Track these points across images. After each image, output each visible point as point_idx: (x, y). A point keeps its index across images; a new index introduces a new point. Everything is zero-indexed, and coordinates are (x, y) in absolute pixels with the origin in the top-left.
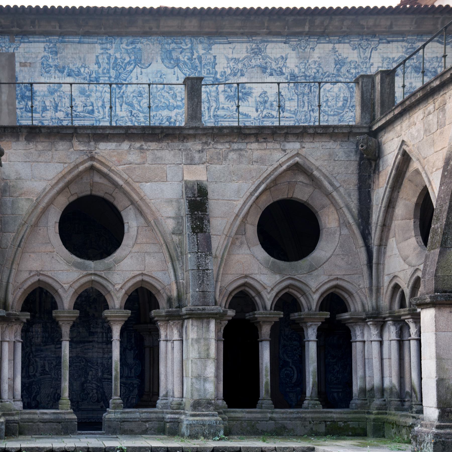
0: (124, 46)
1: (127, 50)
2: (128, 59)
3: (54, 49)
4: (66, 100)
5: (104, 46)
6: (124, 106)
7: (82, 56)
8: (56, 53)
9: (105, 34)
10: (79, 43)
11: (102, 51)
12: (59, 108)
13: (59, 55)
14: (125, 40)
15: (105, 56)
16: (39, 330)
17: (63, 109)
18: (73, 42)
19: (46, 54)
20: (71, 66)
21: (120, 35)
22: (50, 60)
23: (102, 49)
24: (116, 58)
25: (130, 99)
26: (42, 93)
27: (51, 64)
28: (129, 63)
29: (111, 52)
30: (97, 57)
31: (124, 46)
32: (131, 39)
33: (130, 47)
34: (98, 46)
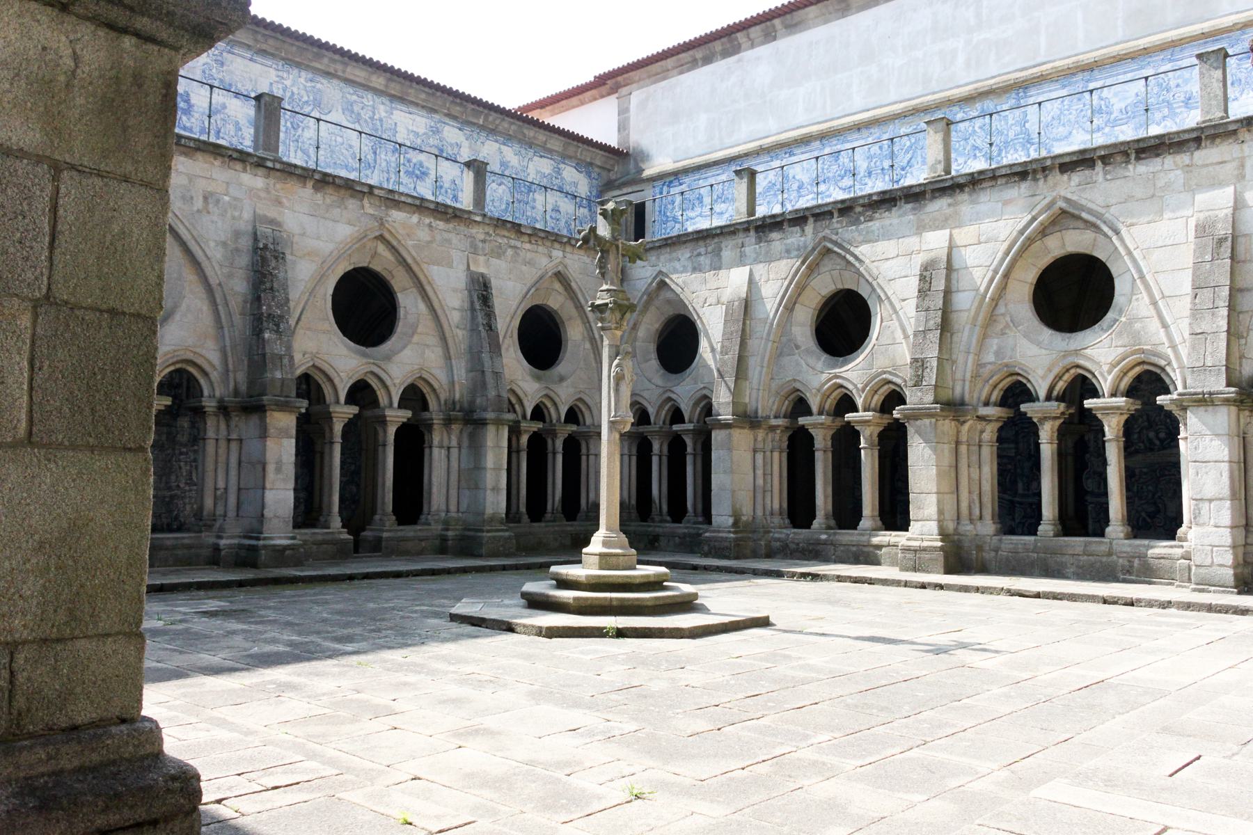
0: (302, 80)
1: (305, 86)
2: (305, 98)
3: (219, 58)
4: (231, 126)
5: (280, 73)
6: (299, 152)
7: (253, 77)
8: (222, 64)
9: (283, 59)
10: (251, 60)
11: (277, 79)
12: (221, 135)
13: (225, 68)
14: (303, 74)
15: (280, 86)
16: (186, 425)
17: (226, 137)
18: (243, 57)
19: (209, 61)
20: (239, 85)
21: (298, 65)
22: (214, 71)
23: (278, 76)
24: (293, 93)
25: (306, 146)
26: (201, 110)
27: (215, 76)
28: (307, 102)
29: (288, 83)
30: (271, 84)
31: (302, 80)
32: (310, 76)
33: (309, 84)
34: (273, 72)
